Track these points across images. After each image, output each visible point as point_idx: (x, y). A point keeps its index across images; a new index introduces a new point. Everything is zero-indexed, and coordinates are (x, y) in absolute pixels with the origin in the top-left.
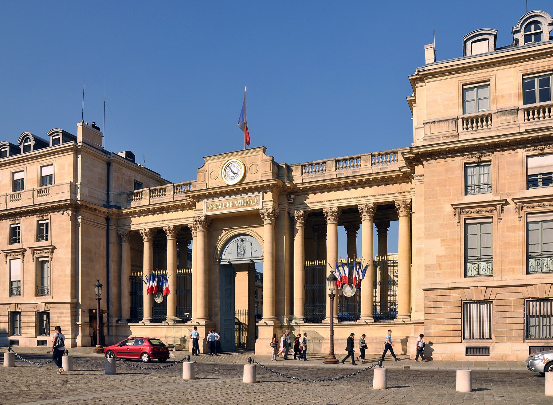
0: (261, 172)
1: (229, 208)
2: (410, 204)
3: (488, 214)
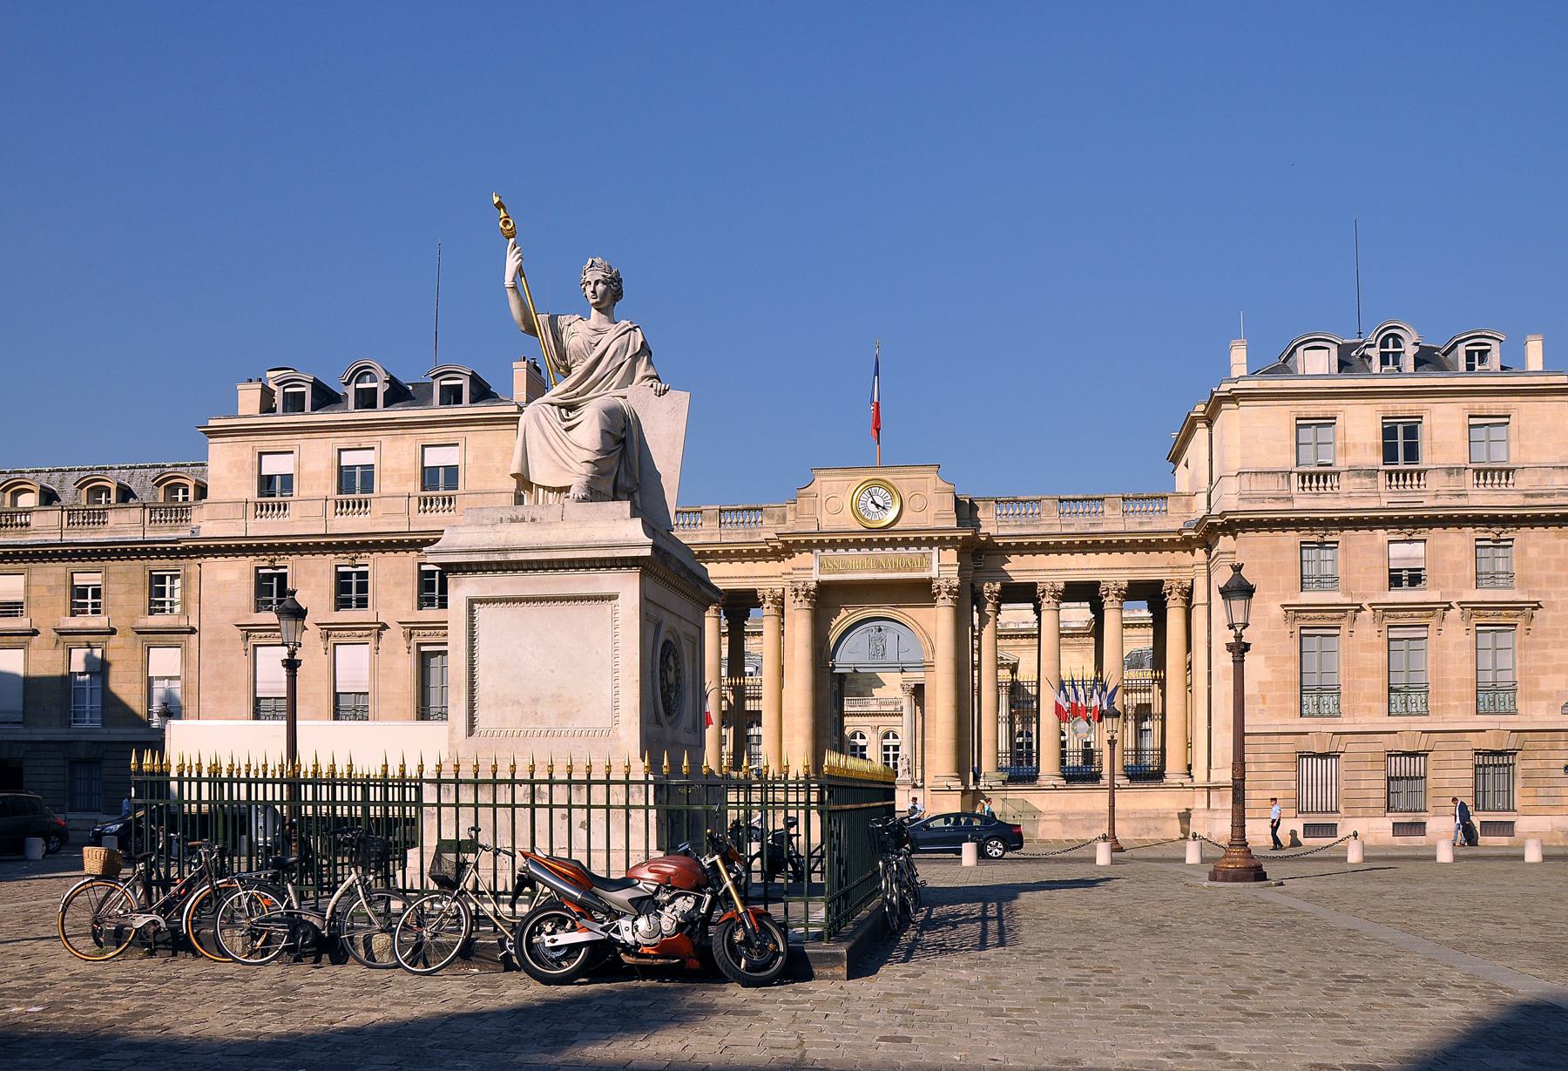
0: (933, 510)
1: (869, 570)
2: (1191, 589)
3: (1334, 623)
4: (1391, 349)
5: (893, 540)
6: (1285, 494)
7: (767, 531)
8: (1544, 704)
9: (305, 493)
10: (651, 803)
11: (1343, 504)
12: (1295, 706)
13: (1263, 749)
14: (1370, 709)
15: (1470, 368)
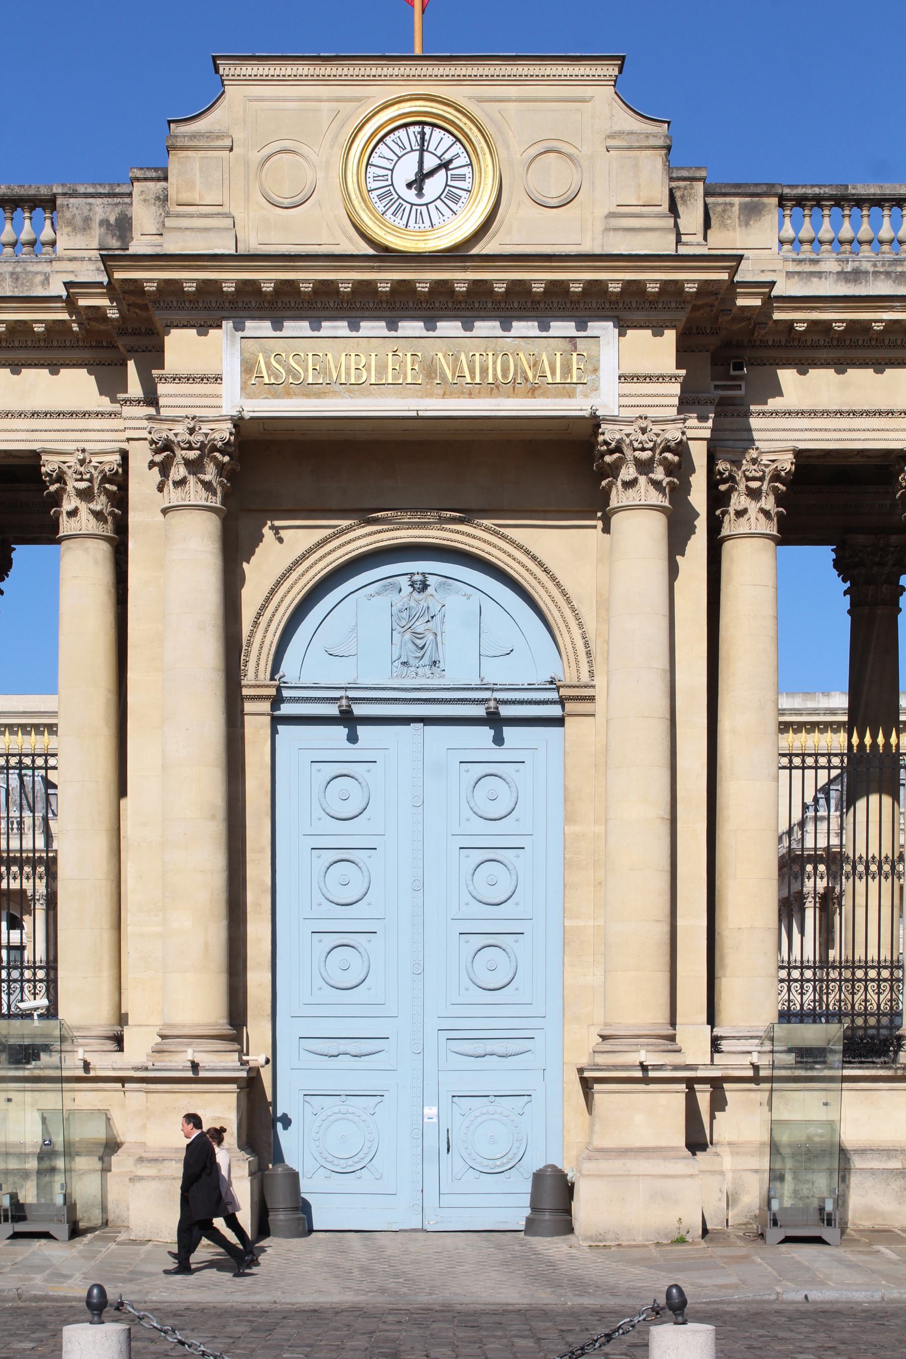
0: (599, 201)
5: (480, 289)
7: (68, 261)
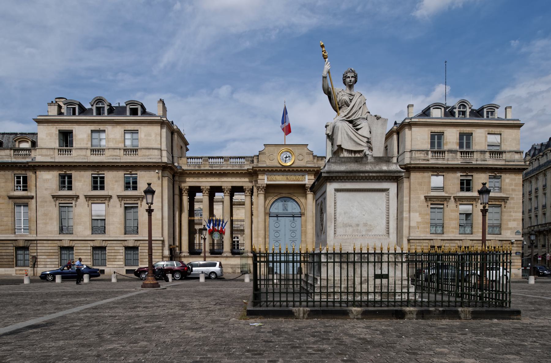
0: (306, 160)
1: (284, 181)
4: (462, 110)
6: (426, 158)
8: (509, 231)
9: (78, 146)
10: (258, 264)
11: (445, 162)
12: (428, 230)
13: (418, 244)
14: (453, 232)
15: (488, 117)
